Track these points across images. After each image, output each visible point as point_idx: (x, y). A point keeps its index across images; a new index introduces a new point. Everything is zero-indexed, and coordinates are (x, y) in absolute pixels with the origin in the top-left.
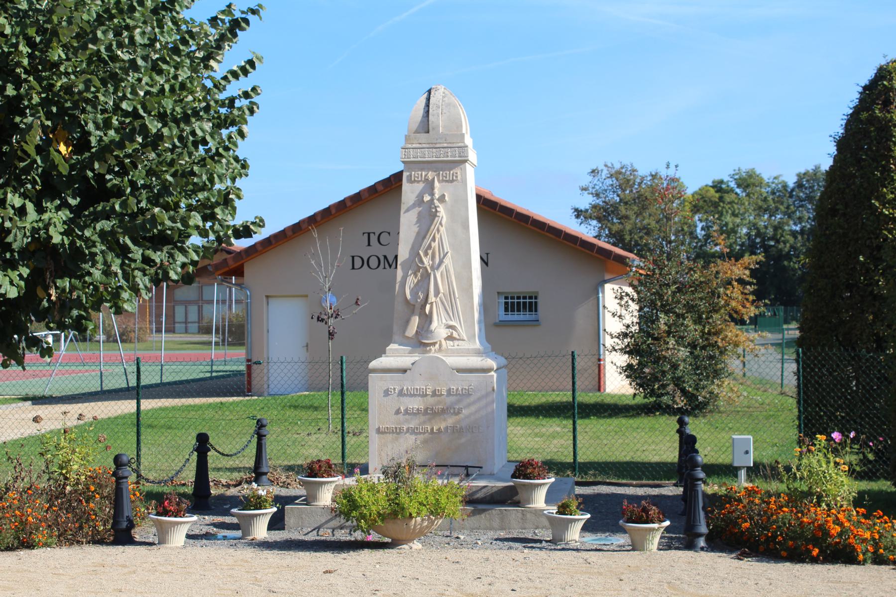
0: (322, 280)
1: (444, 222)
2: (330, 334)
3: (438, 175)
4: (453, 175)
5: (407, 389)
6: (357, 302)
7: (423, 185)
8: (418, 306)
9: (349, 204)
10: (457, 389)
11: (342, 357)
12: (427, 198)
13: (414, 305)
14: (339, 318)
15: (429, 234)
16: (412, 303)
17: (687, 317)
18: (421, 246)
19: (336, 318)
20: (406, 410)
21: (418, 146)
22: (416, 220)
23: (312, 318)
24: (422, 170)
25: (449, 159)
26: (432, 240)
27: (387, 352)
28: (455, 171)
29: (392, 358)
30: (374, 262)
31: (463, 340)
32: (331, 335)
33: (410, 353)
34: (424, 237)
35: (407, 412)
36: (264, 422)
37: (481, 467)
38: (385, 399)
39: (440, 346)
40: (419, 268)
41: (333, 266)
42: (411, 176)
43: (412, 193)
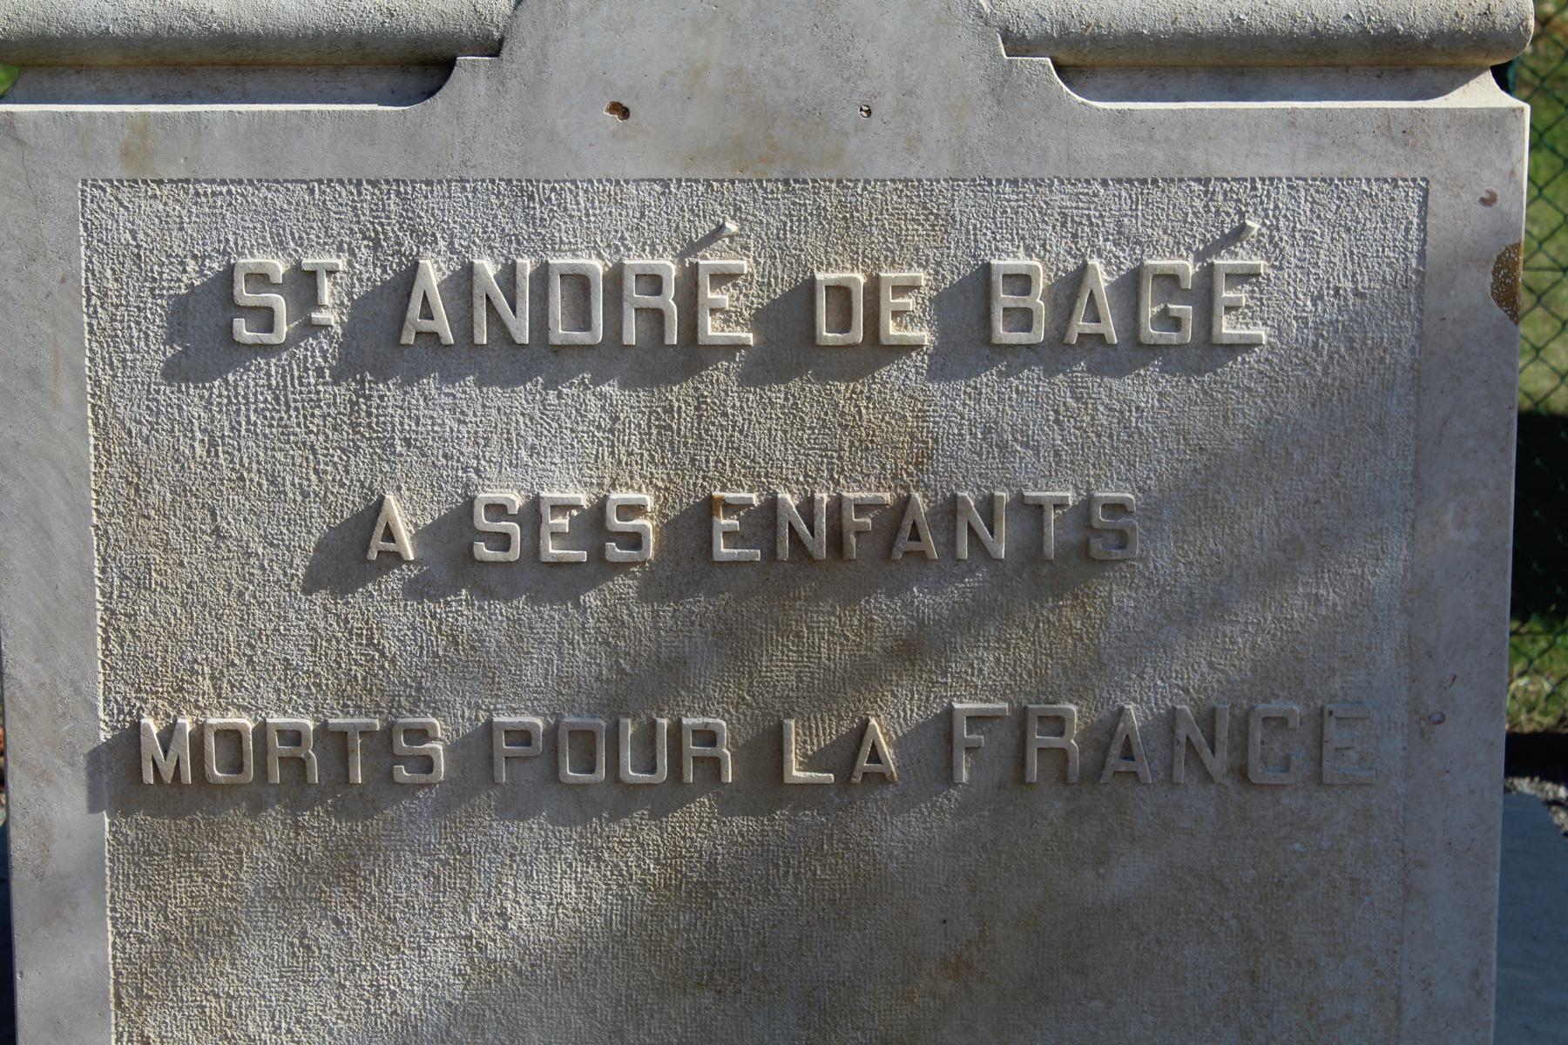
5: (463, 281)
38: (192, 401)
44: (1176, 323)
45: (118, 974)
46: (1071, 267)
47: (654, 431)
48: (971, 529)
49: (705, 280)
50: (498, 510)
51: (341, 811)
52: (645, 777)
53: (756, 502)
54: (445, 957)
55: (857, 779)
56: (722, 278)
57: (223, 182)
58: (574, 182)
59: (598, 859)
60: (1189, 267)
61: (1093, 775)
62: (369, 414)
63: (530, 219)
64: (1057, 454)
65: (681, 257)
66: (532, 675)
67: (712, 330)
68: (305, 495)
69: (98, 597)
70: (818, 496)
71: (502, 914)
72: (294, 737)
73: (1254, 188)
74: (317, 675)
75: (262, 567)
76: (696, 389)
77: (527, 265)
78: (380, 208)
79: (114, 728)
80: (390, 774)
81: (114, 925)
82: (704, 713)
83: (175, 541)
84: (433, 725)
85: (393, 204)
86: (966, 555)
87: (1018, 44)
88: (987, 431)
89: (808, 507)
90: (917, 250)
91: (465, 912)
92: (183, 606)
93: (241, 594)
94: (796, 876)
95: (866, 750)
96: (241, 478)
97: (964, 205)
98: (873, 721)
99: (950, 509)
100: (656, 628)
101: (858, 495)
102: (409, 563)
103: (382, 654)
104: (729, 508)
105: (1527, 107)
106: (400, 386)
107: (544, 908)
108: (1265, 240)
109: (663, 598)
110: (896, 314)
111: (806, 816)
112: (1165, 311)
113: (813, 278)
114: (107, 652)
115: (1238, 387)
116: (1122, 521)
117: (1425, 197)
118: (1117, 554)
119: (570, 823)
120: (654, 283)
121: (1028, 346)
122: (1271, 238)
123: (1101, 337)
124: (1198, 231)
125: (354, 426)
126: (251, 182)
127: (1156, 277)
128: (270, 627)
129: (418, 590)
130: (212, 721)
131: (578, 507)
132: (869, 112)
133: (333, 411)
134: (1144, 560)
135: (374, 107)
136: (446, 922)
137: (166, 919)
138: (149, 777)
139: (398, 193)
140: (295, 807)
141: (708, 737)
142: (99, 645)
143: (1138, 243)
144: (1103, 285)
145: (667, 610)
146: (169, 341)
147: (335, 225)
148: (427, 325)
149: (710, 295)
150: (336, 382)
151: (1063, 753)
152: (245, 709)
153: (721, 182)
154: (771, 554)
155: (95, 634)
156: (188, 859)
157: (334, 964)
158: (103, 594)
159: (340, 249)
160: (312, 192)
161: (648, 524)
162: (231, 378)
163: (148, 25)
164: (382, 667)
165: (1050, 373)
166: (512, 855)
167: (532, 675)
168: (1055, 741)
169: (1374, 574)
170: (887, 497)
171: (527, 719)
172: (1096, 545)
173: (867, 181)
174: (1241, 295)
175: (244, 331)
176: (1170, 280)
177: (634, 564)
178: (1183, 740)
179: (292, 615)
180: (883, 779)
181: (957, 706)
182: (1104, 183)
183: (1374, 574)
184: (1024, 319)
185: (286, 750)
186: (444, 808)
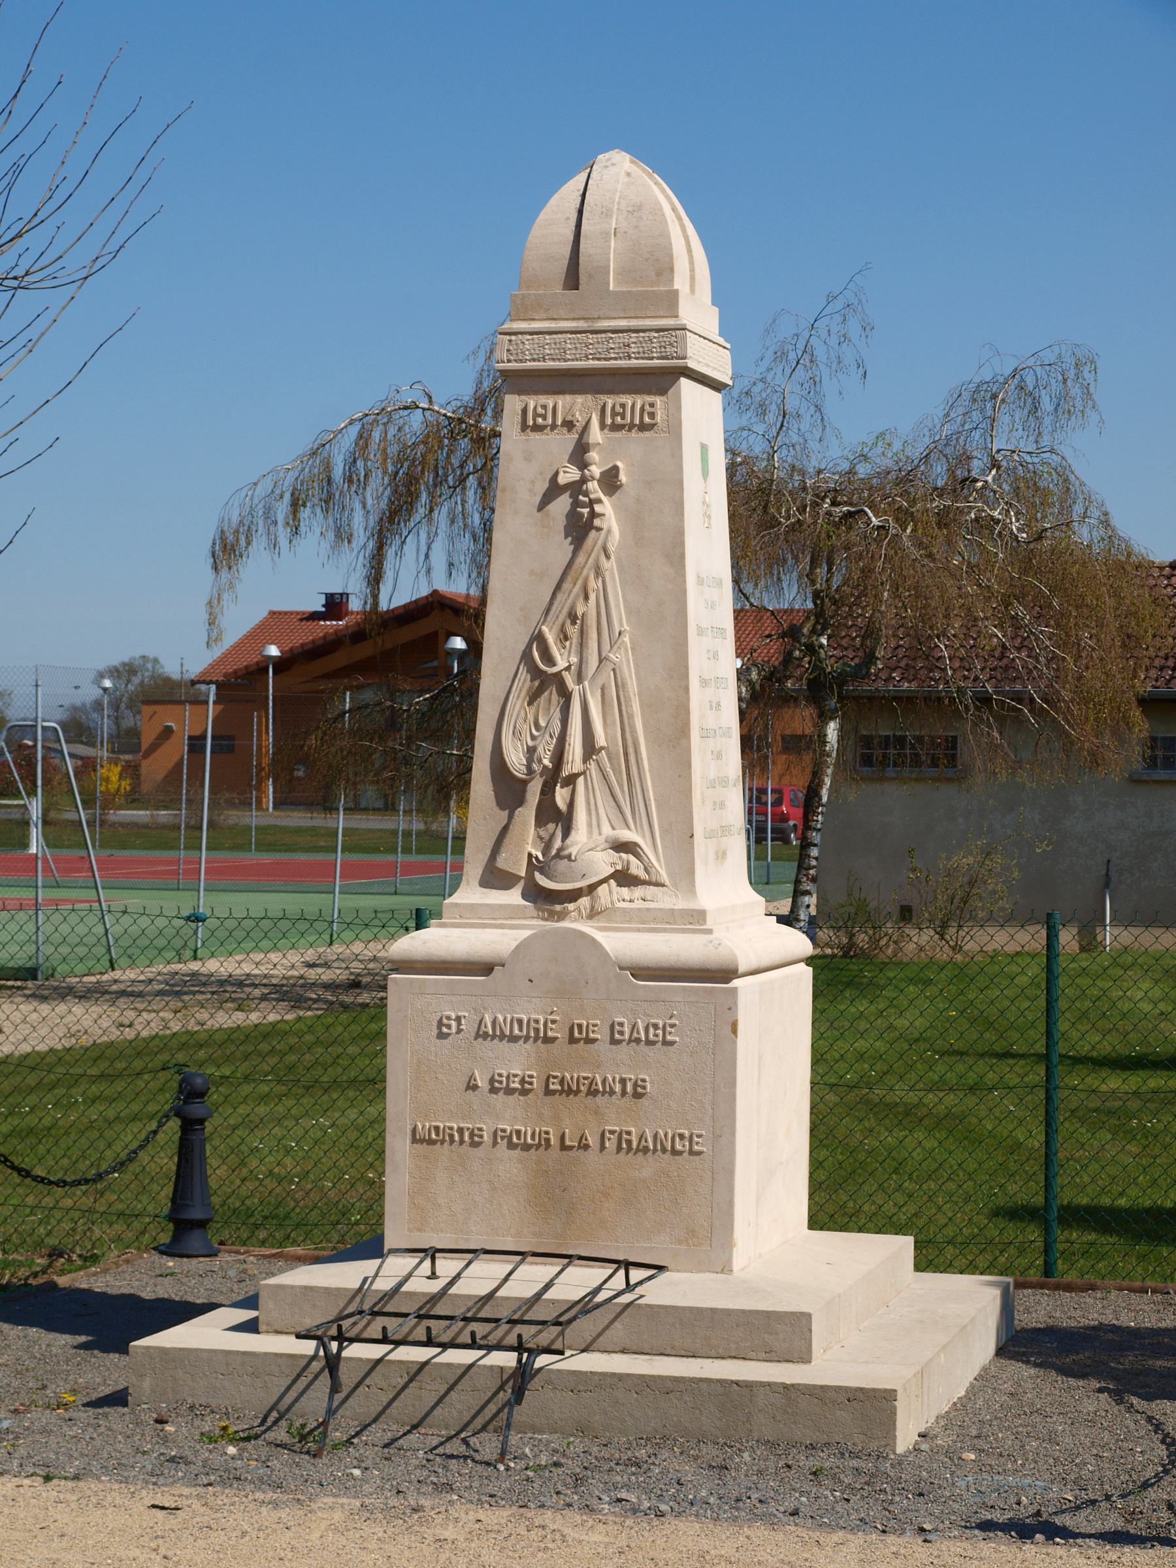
10: (634, 1027)
25: (634, 362)
31: (663, 885)
43: (528, 458)
50: (500, 1075)
72: (451, 1128)
87: (621, 968)
89: (572, 1078)
120: (537, 1021)
148: (486, 1030)
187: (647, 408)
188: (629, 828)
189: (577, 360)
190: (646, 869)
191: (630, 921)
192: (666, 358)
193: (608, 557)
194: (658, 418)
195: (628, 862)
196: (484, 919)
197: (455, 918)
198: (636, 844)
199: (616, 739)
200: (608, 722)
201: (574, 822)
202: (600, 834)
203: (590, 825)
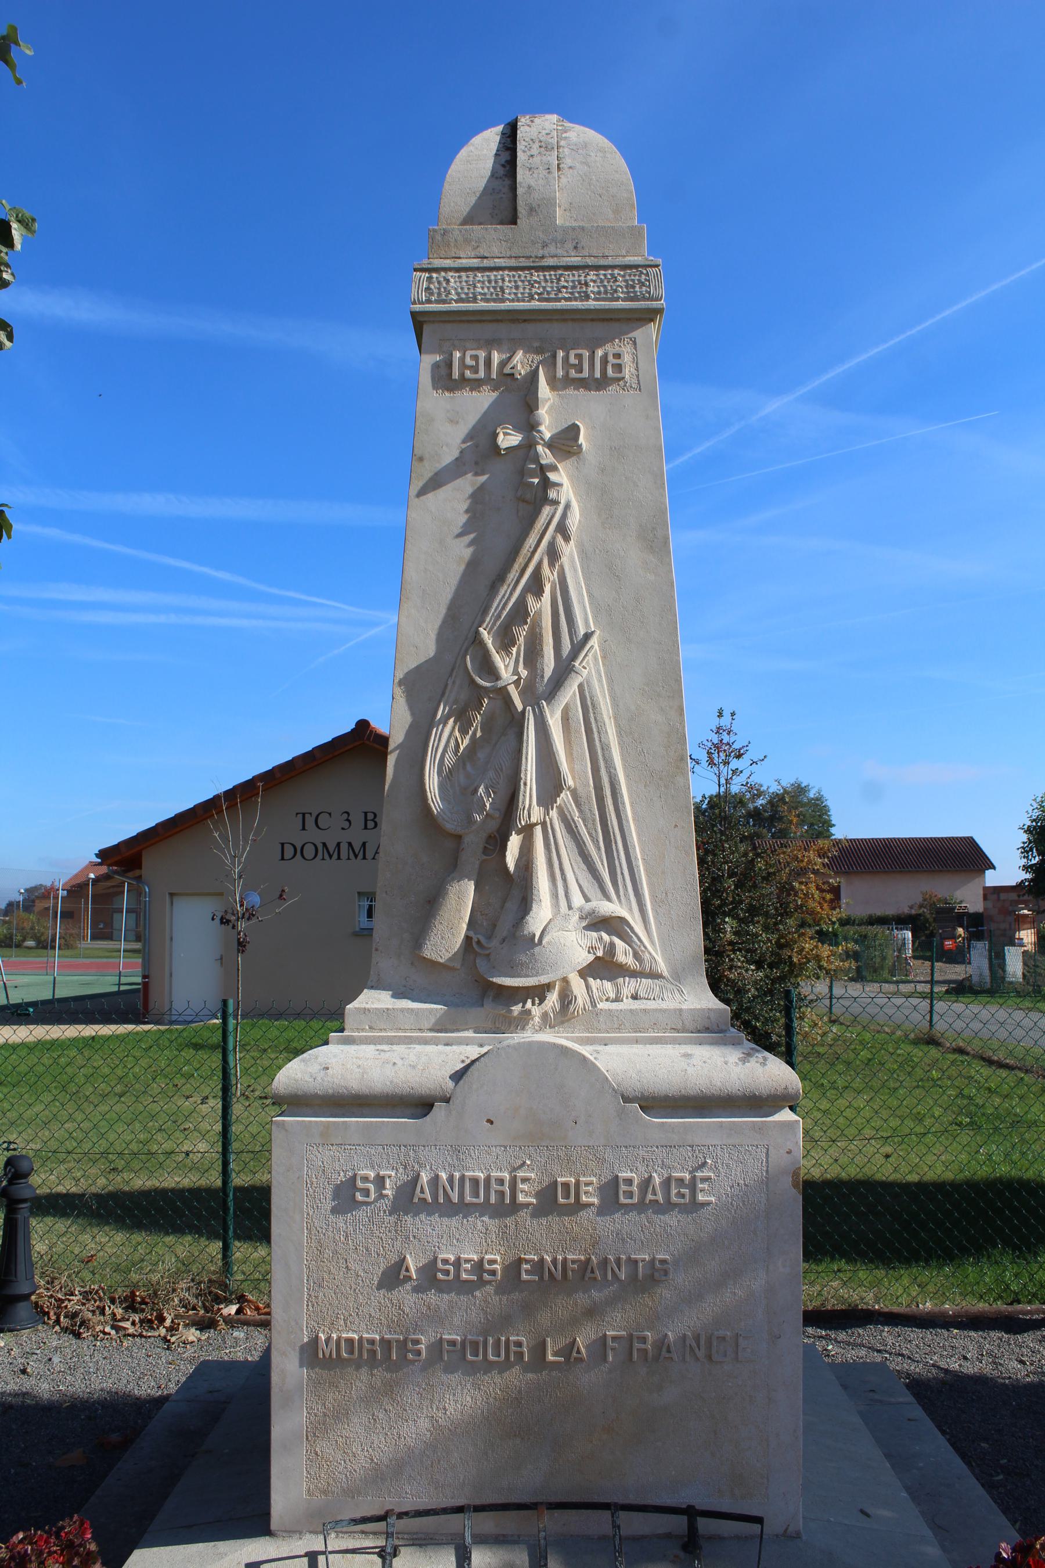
0: (228, 862)
1: (574, 520)
2: (240, 943)
3: (551, 363)
4: (605, 360)
5: (435, 1180)
6: (281, 896)
7: (495, 395)
8: (473, 842)
9: (278, 775)
10: (647, 1182)
11: (225, 1002)
12: (509, 439)
13: (459, 838)
14: (254, 921)
15: (517, 567)
16: (449, 827)
17: (758, 922)
18: (485, 611)
19: (249, 919)
20: (430, 1270)
21: (475, 262)
22: (463, 518)
23: (213, 919)
24: (490, 344)
25: (591, 304)
26: (526, 590)
27: (349, 1021)
28: (610, 348)
29: (369, 1050)
30: (309, 851)
31: (655, 976)
32: (241, 945)
33: (440, 1027)
34: (500, 578)
35: (430, 1273)
36: (24, 1165)
37: (759, 1520)
38: (340, 1221)
39: (566, 998)
40: (478, 693)
41: (246, 840)
42: (449, 365)
43: (453, 421)
44: (683, 1196)
45: (307, 1427)
46: (646, 1176)
47: (501, 1234)
48: (612, 1269)
49: (519, 1181)
50: (445, 1261)
51: (387, 1370)
52: (496, 1359)
53: (536, 1259)
54: (424, 1424)
55: (572, 1360)
56: (525, 1180)
57: (354, 1145)
58: (474, 1146)
59: (479, 1389)
60: (687, 1176)
61: (657, 1358)
62: (401, 1227)
63: (458, 1159)
64: (642, 1242)
65: (510, 1173)
66: (456, 1321)
67: (521, 1198)
68: (378, 1255)
69: (306, 1290)
70: (558, 1257)
71: (445, 1409)
72: (372, 1342)
73: (709, 1149)
74: (381, 1320)
75: (362, 1280)
76: (515, 1219)
77: (457, 1175)
78: (407, 1155)
79: (309, 1337)
80: (406, 1356)
81: (307, 1410)
82: (517, 1335)
83: (333, 1270)
84: (421, 1339)
85: (411, 1153)
86: (610, 1279)
87: (627, 1099)
88: (617, 1234)
89: (554, 1261)
90: (593, 1170)
91: (431, 1407)
92: (335, 1294)
93: (355, 1290)
94: (550, 1395)
95: (576, 1349)
96: (356, 1248)
97: (609, 1155)
98: (578, 1339)
99: (605, 1262)
100: (500, 1304)
101: (572, 1257)
102: (414, 1280)
103: (404, 1313)
104: (527, 1261)
105: (801, 1119)
106: (412, 1217)
107: (459, 1406)
108: (713, 1167)
109: (503, 1293)
110: (585, 1193)
111: (554, 1373)
112: (679, 1191)
113: (556, 1180)
114: (308, 1310)
115: (705, 1218)
116: (665, 1266)
117: (768, 1151)
118: (664, 1278)
119: (469, 1375)
120: (501, 1181)
121: (632, 1204)
122: (715, 1166)
123: (657, 1201)
124: (690, 1164)
125: (396, 1231)
126: (363, 1145)
127: (676, 1180)
128: (365, 1302)
129: (417, 1290)
130: (343, 1335)
131: (474, 1261)
132: (576, 1123)
133: (389, 1225)
134: (674, 1280)
135: (406, 1120)
136: (425, 1411)
137: (325, 1408)
138: (321, 1356)
139: (413, 1149)
140: (372, 1367)
141: (519, 1344)
142: (305, 1307)
143: (669, 1168)
144: (657, 1182)
145: (504, 1298)
146: (333, 1200)
147: (391, 1161)
148: (422, 1196)
149: (521, 1186)
150: (390, 1215)
151: (646, 1351)
152: (356, 1332)
153: (525, 1147)
154: (541, 1278)
155: (304, 1303)
156: (333, 1386)
157: (384, 1426)
158: (307, 1289)
159: (393, 1169)
160: (384, 1149)
161: (498, 1267)
162: (354, 1213)
163: (331, 1091)
164: (403, 1317)
165: (639, 1214)
166: (448, 1387)
167: (456, 1321)
168: (642, 1346)
169: (754, 1284)
170: (583, 1258)
171: (454, 1337)
172: (656, 1275)
173: (575, 1147)
174: (705, 1186)
175: (359, 1197)
176: (680, 1181)
177: (493, 1281)
178: (688, 1345)
179: (372, 1298)
180: (581, 1360)
181: (607, 1333)
182: (657, 1147)
183: (754, 1284)
184: (630, 1195)
185: (369, 1347)
186: (424, 1369)
187: (610, 358)
188: (609, 899)
189: (518, 301)
190: (636, 956)
191: (619, 1029)
192: (632, 299)
193: (567, 538)
194: (628, 372)
195: (612, 945)
196: (405, 1031)
197: (363, 1030)
198: (622, 920)
199: (587, 777)
200: (575, 754)
201: (535, 892)
202: (570, 908)
203: (555, 895)
